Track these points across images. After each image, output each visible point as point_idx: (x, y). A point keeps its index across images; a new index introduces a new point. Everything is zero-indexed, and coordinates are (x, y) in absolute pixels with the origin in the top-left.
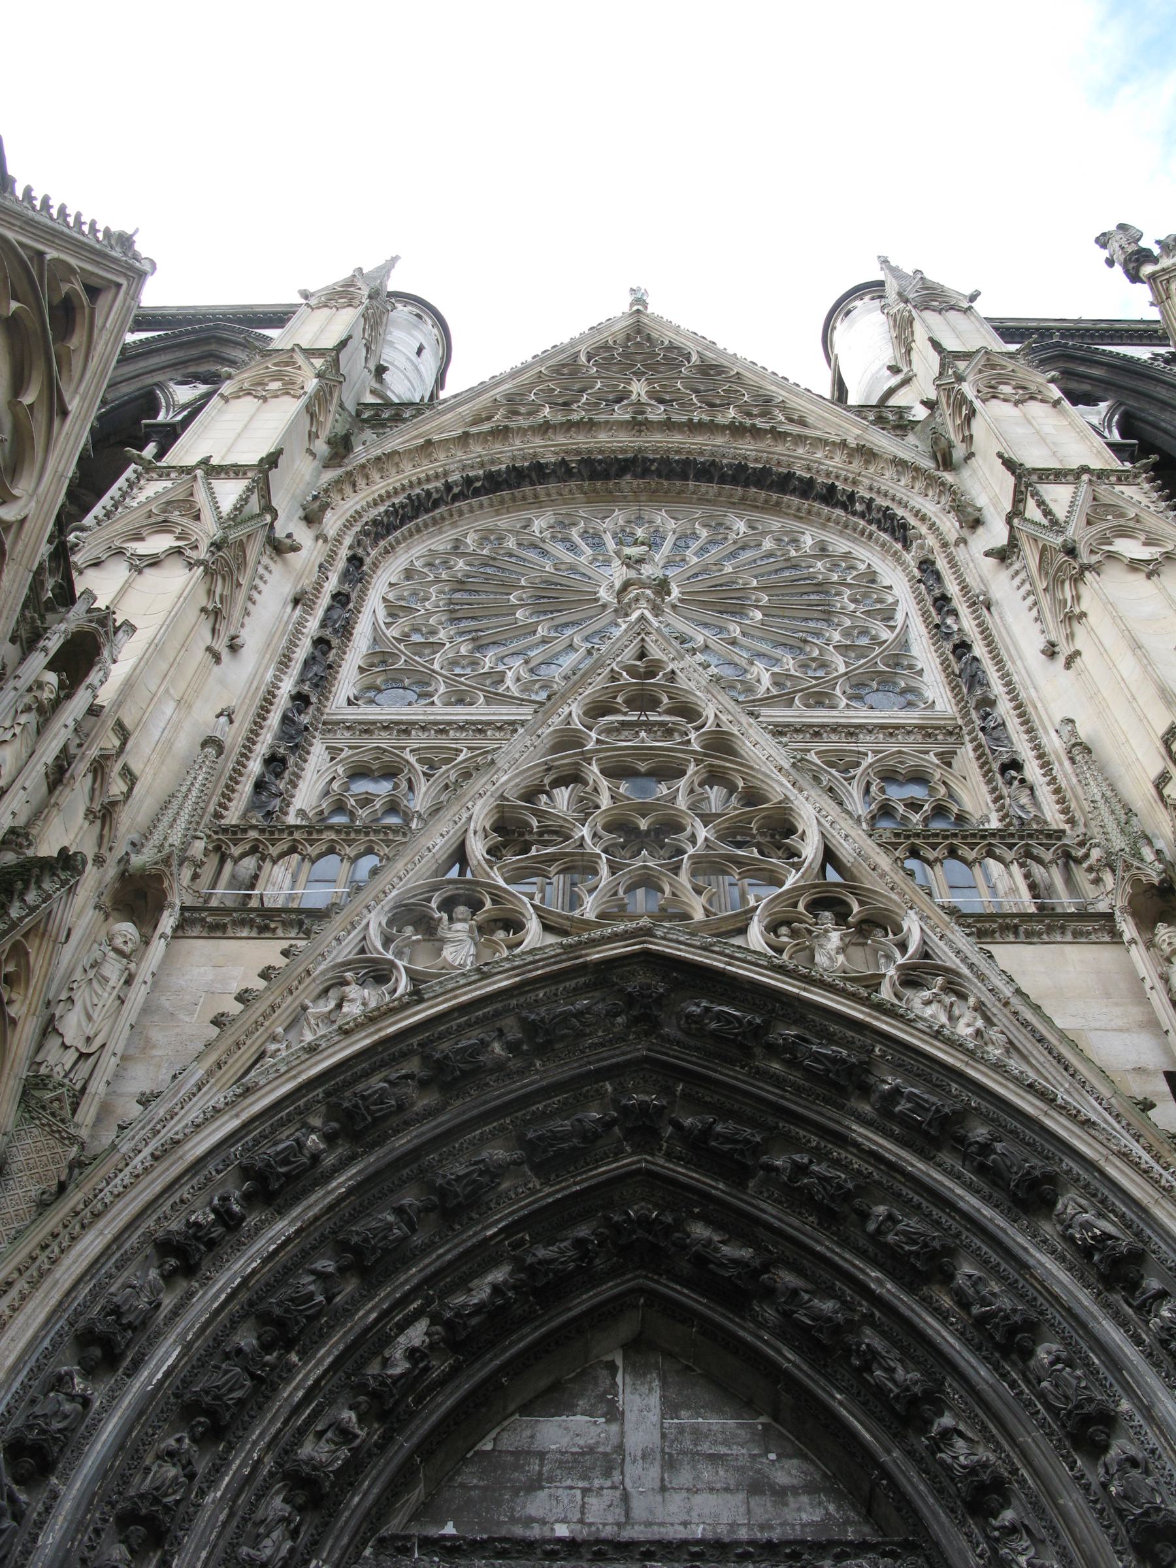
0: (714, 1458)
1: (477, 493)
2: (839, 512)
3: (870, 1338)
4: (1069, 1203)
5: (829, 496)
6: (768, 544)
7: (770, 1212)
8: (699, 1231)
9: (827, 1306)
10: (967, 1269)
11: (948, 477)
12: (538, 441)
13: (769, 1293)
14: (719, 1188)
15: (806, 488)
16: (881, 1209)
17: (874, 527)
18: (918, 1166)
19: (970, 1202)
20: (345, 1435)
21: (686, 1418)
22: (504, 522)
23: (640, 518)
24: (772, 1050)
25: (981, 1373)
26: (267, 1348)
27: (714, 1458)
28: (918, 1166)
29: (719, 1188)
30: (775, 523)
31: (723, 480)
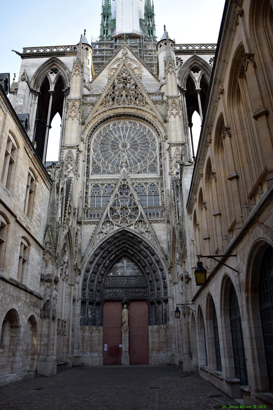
0: (131, 267)
1: (102, 122)
2: (151, 126)
3: (142, 261)
4: (155, 256)
5: (150, 123)
6: (142, 131)
7: (134, 250)
8: (129, 251)
9: (138, 258)
10: (148, 258)
11: (165, 124)
12: (110, 111)
13: (135, 256)
14: (131, 248)
15: (147, 121)
16: (143, 252)
17: (155, 130)
18: (145, 250)
19: (149, 254)
20: (104, 271)
21: (129, 263)
22: (106, 125)
23: (125, 122)
24: (135, 238)
25: (149, 266)
26: (98, 267)
27: (131, 267)
28: (145, 250)
29: (131, 248)
30: (143, 124)
31: (136, 117)
